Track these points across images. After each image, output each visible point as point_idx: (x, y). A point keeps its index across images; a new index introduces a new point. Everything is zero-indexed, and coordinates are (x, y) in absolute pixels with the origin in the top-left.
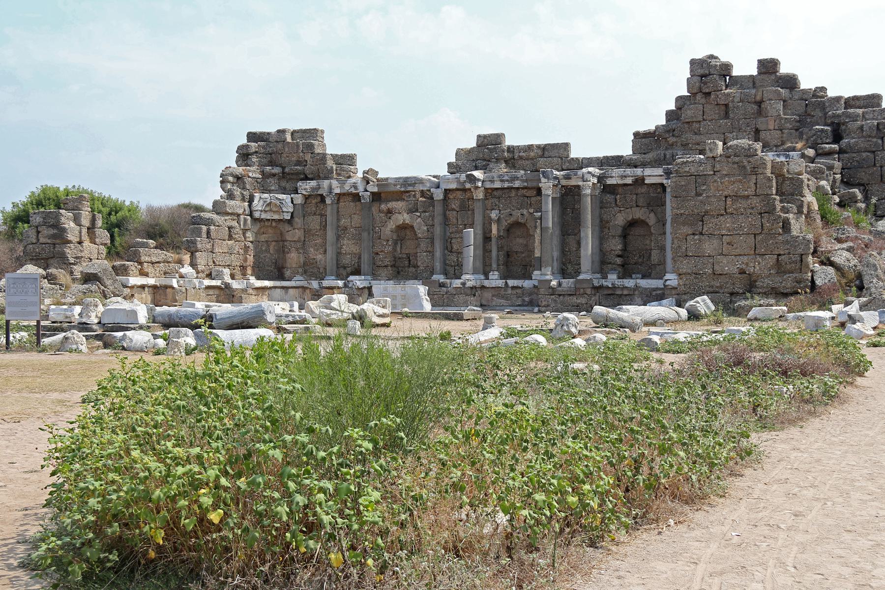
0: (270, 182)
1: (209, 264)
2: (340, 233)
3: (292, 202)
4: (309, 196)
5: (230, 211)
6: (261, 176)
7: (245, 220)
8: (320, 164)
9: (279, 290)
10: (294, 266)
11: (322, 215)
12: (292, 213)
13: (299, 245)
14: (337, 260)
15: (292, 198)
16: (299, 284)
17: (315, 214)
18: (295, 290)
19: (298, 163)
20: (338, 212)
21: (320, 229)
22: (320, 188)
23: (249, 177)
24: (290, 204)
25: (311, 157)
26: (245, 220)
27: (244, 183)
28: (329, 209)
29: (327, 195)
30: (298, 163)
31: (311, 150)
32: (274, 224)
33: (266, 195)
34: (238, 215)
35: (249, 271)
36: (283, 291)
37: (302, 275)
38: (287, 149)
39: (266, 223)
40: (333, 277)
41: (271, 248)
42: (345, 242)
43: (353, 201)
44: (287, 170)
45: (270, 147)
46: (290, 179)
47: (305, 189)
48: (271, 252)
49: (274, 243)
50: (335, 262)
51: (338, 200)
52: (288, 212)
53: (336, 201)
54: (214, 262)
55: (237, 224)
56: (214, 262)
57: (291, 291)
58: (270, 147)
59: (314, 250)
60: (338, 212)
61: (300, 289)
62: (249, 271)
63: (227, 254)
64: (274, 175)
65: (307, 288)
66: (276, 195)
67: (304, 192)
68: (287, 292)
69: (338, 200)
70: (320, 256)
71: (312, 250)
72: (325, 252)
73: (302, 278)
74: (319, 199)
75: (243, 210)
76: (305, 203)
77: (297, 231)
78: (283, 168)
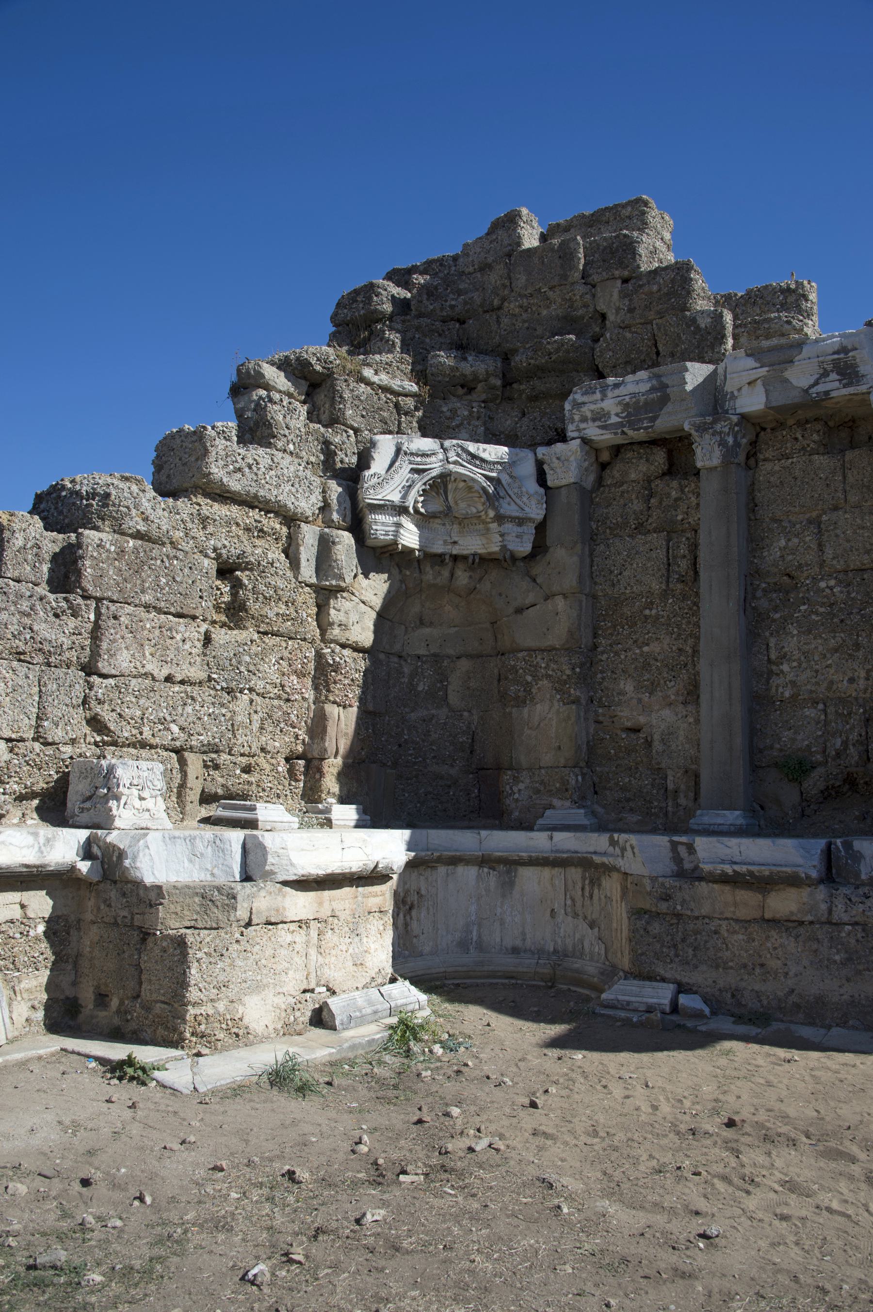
0: (454, 411)
1: (57, 734)
2: (763, 604)
3: (541, 478)
4: (617, 450)
5: (235, 484)
6: (415, 388)
7: (325, 546)
8: (661, 315)
9: (471, 872)
10: (547, 759)
11: (670, 530)
12: (541, 528)
13: (565, 667)
14: (753, 732)
15: (540, 465)
16: (566, 841)
17: (640, 528)
18: (547, 872)
19: (569, 323)
20: (752, 506)
21: (665, 594)
22: (665, 400)
23: (362, 380)
24: (532, 486)
25: (624, 295)
26: (325, 546)
27: (334, 397)
28: (710, 486)
29: (702, 428)
30: (569, 323)
31: (622, 265)
32: (463, 578)
33: (427, 444)
34: (291, 520)
35: (330, 783)
36: (492, 879)
37: (580, 801)
38: (521, 280)
39: (429, 575)
40: (733, 817)
41: (455, 684)
42: (792, 642)
43: (826, 448)
44: (521, 360)
45: (459, 293)
46: (534, 398)
47: (599, 417)
48: (454, 699)
49: (464, 665)
50: (739, 741)
51: (752, 454)
52: (521, 521)
53: (742, 458)
54: (96, 723)
55: (276, 554)
56: (96, 723)
57: (529, 878)
58: (459, 293)
59: (638, 688)
60: (752, 506)
61: (575, 873)
62: (330, 783)
63: (204, 694)
64: (468, 386)
65: (609, 869)
66: (472, 447)
67: (593, 432)
68: (507, 885)
69: (752, 454)
70: (666, 713)
71: (628, 686)
72: (692, 694)
73: (579, 815)
74: (660, 457)
75: (316, 499)
76: (600, 481)
77: (560, 603)
78: (506, 358)
